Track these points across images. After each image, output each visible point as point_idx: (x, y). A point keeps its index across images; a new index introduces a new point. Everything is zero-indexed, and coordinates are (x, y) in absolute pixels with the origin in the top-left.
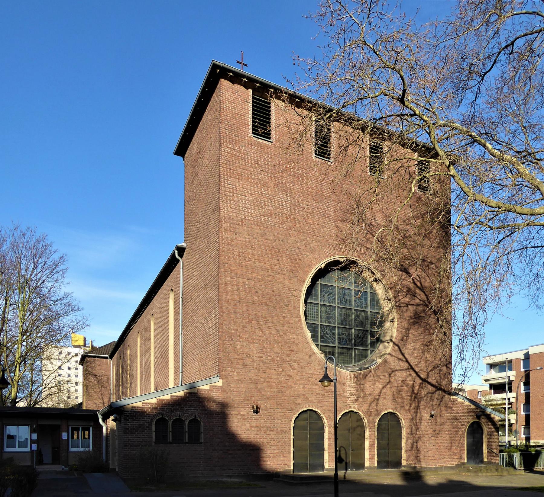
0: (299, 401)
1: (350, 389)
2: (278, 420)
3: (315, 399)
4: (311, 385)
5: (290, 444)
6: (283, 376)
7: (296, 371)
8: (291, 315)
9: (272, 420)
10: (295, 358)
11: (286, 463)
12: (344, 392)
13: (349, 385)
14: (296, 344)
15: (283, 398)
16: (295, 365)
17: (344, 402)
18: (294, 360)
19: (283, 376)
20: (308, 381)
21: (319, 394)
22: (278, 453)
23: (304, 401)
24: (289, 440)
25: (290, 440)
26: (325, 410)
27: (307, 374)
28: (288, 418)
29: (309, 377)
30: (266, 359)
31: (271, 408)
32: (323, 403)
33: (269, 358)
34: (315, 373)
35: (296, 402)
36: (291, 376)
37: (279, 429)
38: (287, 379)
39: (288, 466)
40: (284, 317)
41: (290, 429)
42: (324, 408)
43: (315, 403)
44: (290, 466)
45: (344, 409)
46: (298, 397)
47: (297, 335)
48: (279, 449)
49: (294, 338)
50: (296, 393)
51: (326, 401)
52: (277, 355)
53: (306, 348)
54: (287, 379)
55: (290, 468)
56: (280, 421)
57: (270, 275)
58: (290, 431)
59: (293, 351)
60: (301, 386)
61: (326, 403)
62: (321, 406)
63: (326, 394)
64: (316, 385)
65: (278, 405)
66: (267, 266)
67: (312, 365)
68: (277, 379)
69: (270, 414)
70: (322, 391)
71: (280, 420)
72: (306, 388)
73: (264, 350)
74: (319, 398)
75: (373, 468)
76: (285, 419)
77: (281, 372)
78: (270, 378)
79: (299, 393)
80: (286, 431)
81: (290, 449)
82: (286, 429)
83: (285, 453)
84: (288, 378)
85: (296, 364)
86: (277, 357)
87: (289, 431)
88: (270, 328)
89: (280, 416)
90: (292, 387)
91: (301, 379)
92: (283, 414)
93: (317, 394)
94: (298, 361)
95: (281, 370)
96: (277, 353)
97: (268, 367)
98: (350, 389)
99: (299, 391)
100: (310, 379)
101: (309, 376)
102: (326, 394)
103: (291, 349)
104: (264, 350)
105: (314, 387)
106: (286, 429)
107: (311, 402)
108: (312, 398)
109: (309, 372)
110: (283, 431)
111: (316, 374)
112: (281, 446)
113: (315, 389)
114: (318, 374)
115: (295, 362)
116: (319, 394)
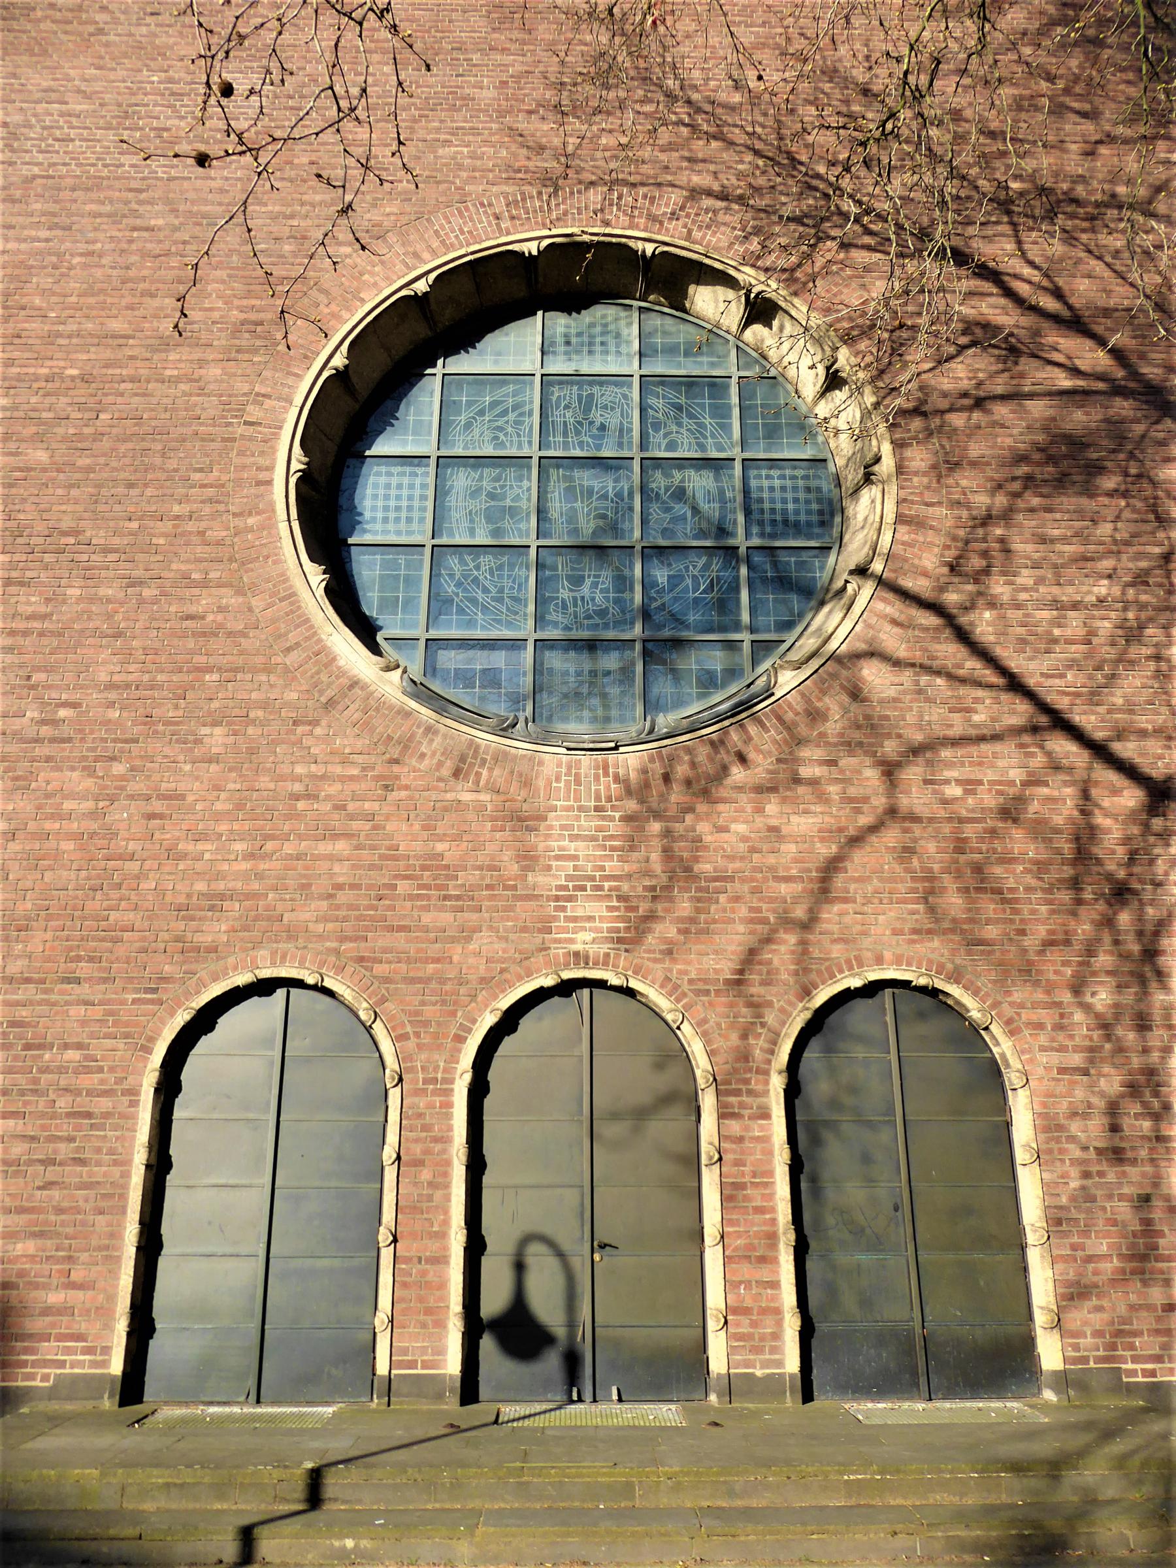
0: (215, 930)
1: (572, 847)
2: (66, 1046)
3: (325, 919)
4: (301, 838)
5: (123, 1197)
6: (131, 797)
7: (214, 767)
8: (221, 507)
9: (27, 1047)
10: (215, 705)
11: (83, 1327)
12: (526, 869)
13: (563, 827)
14: (230, 634)
15: (113, 916)
16: (216, 738)
17: (524, 929)
18: (210, 713)
19: (131, 797)
20: (288, 817)
21: (353, 886)
22: (32, 1258)
23: (246, 929)
24: (116, 1171)
25: (126, 1175)
26: (387, 980)
27: (282, 778)
28: (127, 1036)
29: (297, 797)
30: (44, 722)
31: (28, 981)
32: (381, 940)
33: (63, 713)
34: (338, 770)
35: (198, 938)
36: (182, 797)
37: (63, 1104)
38: (151, 816)
39: (89, 1351)
40: (177, 517)
41: (134, 1104)
42: (379, 969)
43: (321, 937)
44: (107, 1350)
45: (529, 974)
46: (212, 908)
47: (240, 592)
48: (41, 1235)
49: (222, 609)
50: (201, 886)
51: (401, 929)
52: (112, 695)
53: (289, 650)
54: (151, 816)
55: (105, 1364)
56: (73, 1055)
57: (132, 358)
58: (134, 1117)
59: (209, 670)
60: (239, 847)
61: (399, 940)
62: (361, 959)
63: (403, 887)
64: (335, 837)
65: (79, 959)
66: (116, 325)
67: (318, 731)
68: (93, 815)
69: (23, 1013)
70: (372, 867)
71: (79, 1046)
72: (268, 856)
73: (38, 677)
74: (351, 907)
75: (771, 1387)
76: (109, 1043)
77: (122, 778)
78: (52, 817)
79: (221, 886)
80: (107, 1115)
81: (116, 1235)
82: (105, 1104)
83: (84, 1257)
84: (158, 806)
85: (218, 731)
86: (111, 705)
87: (122, 1116)
88: (89, 575)
89: (84, 1023)
90: (183, 856)
91: (240, 807)
92: (97, 1012)
93: (339, 887)
94: (236, 721)
95: (119, 768)
96: (111, 686)
97: (48, 759)
98: (572, 847)
99: (219, 876)
100: (301, 805)
101: (298, 787)
102: (403, 887)
103: (200, 660)
104: (38, 677)
105: (324, 848)
106: (105, 1104)
107: (291, 934)
108: (307, 913)
109: (300, 770)
110: (89, 1115)
111: (343, 779)
112: (60, 1211)
113: (331, 858)
114: (352, 778)
115: (215, 724)
116: (353, 886)
